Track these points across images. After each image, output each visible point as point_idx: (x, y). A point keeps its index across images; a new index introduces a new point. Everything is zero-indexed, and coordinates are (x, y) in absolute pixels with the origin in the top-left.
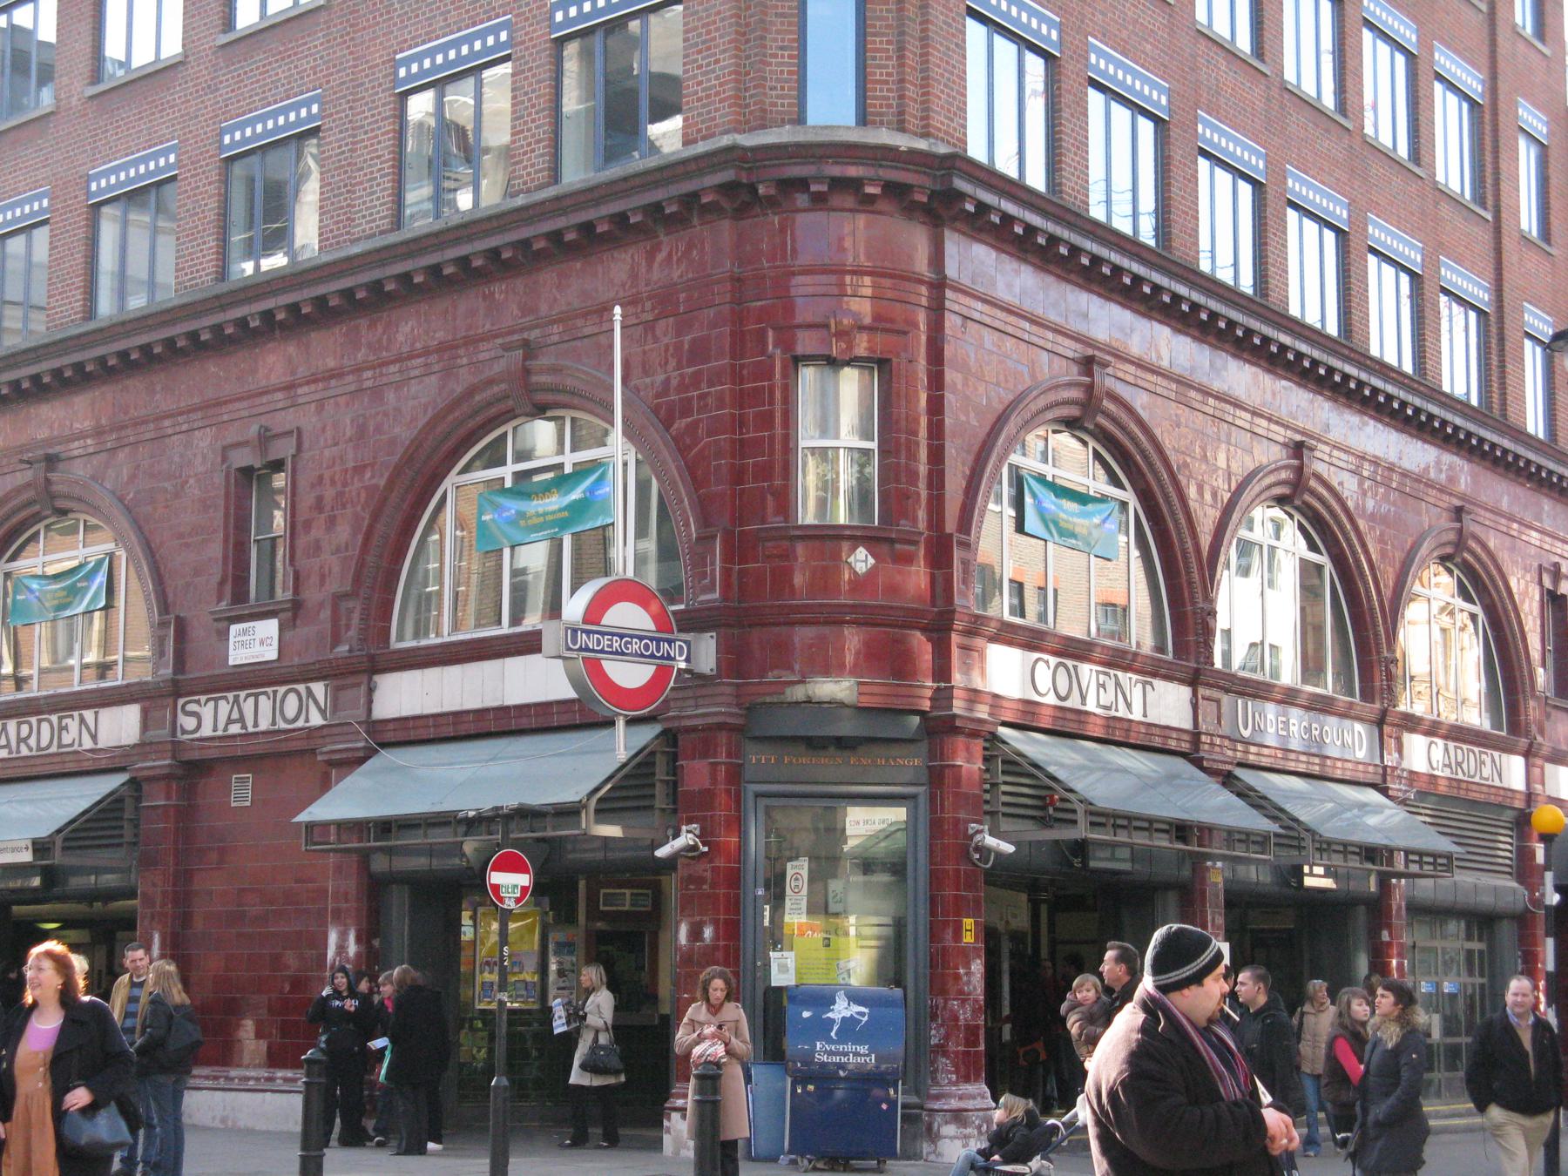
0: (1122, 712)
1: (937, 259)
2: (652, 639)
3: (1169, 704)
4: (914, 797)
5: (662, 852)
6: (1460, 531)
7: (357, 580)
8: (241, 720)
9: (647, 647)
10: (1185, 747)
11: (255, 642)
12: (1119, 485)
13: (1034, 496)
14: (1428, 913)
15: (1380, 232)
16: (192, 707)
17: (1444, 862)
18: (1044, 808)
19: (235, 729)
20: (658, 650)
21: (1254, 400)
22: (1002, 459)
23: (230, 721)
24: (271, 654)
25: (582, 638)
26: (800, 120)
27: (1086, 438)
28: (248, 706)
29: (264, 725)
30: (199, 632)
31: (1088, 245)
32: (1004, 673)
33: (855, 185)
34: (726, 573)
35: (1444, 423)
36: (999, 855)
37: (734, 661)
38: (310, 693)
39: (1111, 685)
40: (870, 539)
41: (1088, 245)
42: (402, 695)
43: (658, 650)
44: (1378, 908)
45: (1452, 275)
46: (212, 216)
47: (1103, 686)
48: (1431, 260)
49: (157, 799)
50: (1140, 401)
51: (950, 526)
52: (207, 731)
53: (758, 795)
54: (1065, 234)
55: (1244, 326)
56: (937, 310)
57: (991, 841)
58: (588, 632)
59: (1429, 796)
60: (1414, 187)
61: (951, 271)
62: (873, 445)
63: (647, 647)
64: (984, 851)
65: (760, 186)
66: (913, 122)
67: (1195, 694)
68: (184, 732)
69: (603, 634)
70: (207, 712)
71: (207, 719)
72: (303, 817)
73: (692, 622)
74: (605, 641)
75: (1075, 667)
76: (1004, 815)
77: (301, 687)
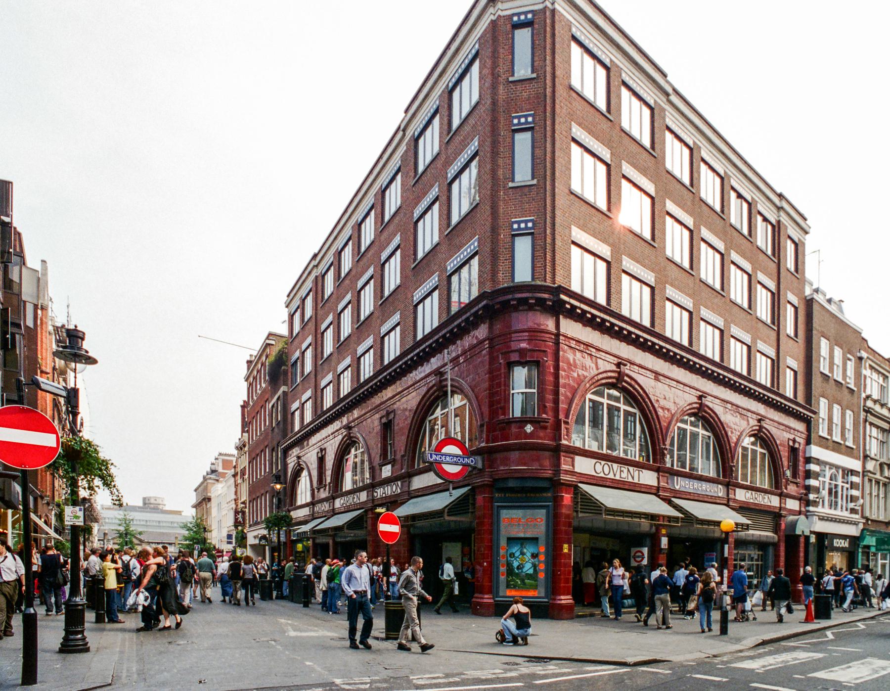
0: (630, 480)
3: (649, 478)
4: (548, 506)
10: (654, 491)
11: (387, 472)
17: (747, 527)
32: (583, 465)
39: (626, 471)
40: (532, 421)
48: (754, 340)
50: (640, 379)
51: (562, 416)
59: (743, 509)
62: (535, 391)
70: (379, 491)
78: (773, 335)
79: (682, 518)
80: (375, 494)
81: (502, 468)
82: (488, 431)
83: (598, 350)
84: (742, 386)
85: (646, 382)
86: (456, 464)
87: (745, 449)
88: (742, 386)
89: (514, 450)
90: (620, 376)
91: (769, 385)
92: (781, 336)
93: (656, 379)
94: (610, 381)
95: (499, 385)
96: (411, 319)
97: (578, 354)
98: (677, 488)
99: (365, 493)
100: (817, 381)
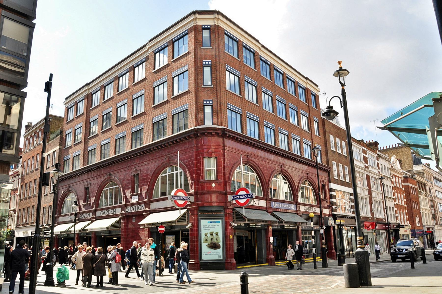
0: (255, 205)
1: (224, 143)
3: (262, 203)
10: (265, 209)
11: (135, 199)
19: (133, 211)
26: (204, 124)
33: (211, 133)
34: (195, 187)
44: (297, 230)
51: (227, 179)
52: (129, 211)
57: (233, 224)
62: (215, 169)
64: (234, 226)
65: (200, 134)
66: (219, 124)
70: (129, 209)
71: (129, 210)
78: (310, 135)
80: (127, 210)
84: (300, 160)
89: (207, 194)
98: (275, 207)
100: (330, 154)
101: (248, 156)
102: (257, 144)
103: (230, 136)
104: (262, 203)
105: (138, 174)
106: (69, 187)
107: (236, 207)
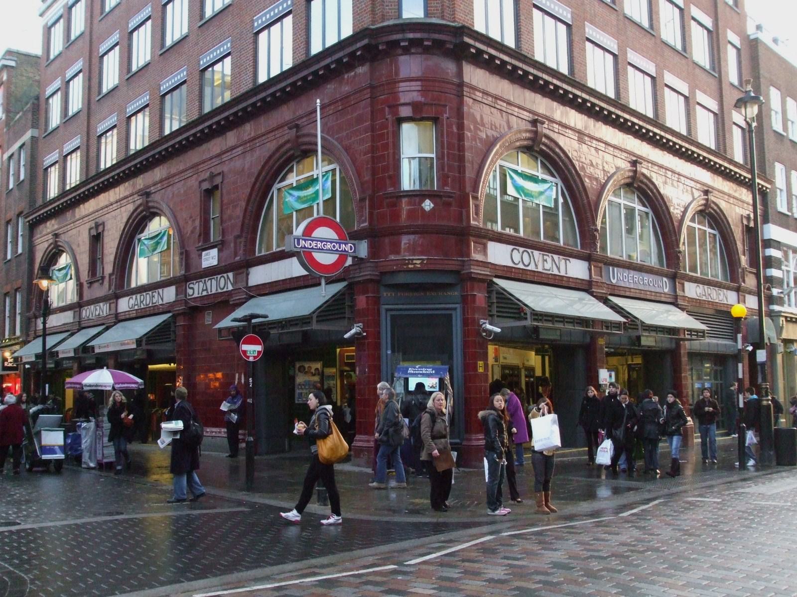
0: (556, 272)
1: (460, 73)
2: (336, 243)
3: (577, 269)
5: (346, 336)
6: (707, 200)
7: (242, 230)
8: (206, 290)
9: (334, 247)
10: (586, 287)
11: (210, 258)
12: (553, 176)
13: (512, 178)
14: (697, 357)
15: (669, 78)
16: (191, 286)
17: (700, 334)
18: (519, 313)
19: (205, 293)
20: (340, 248)
21: (613, 142)
22: (493, 162)
23: (203, 290)
24: (215, 262)
25: (302, 243)
27: (537, 155)
28: (209, 284)
29: (214, 291)
30: (194, 255)
31: (531, 70)
32: (499, 254)
34: (371, 214)
35: (699, 155)
36: (496, 333)
37: (374, 251)
38: (228, 278)
39: (549, 260)
40: (431, 195)
41: (531, 70)
42: (259, 275)
43: (340, 248)
45: (701, 97)
46: (197, 93)
47: (546, 261)
49: (181, 322)
50: (562, 141)
52: (196, 295)
53: (387, 310)
54: (520, 65)
55: (609, 112)
56: (460, 96)
58: (305, 240)
59: (695, 309)
60: (684, 61)
61: (466, 79)
62: (433, 156)
63: (334, 247)
64: (489, 332)
67: (590, 265)
68: (189, 295)
69: (312, 241)
70: (196, 287)
71: (196, 290)
72: (217, 326)
73: (355, 236)
74: (314, 244)
75: (532, 252)
76: (498, 316)
77: (225, 275)
78: (713, 83)
79: (625, 323)
80: (190, 292)
81: (392, 257)
82: (372, 207)
83: (509, 103)
85: (568, 143)
86: (330, 251)
87: (691, 230)
88: (683, 149)
90: (536, 137)
91: (713, 147)
92: (723, 85)
93: (581, 141)
94: (525, 143)
95: (386, 147)
96: (251, 52)
97: (487, 109)
98: (614, 281)
99: (172, 289)
101: (534, 123)
102: (565, 86)
103: (480, 52)
104: (577, 269)
105: (216, 187)
106: (56, 236)
107: (497, 277)
